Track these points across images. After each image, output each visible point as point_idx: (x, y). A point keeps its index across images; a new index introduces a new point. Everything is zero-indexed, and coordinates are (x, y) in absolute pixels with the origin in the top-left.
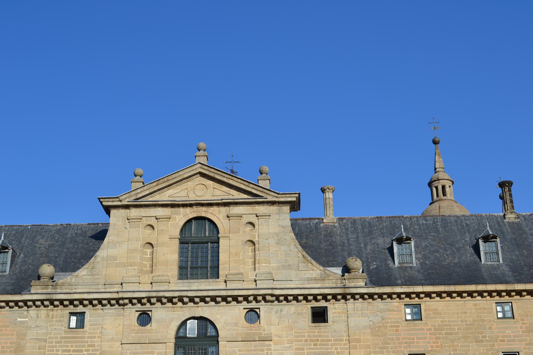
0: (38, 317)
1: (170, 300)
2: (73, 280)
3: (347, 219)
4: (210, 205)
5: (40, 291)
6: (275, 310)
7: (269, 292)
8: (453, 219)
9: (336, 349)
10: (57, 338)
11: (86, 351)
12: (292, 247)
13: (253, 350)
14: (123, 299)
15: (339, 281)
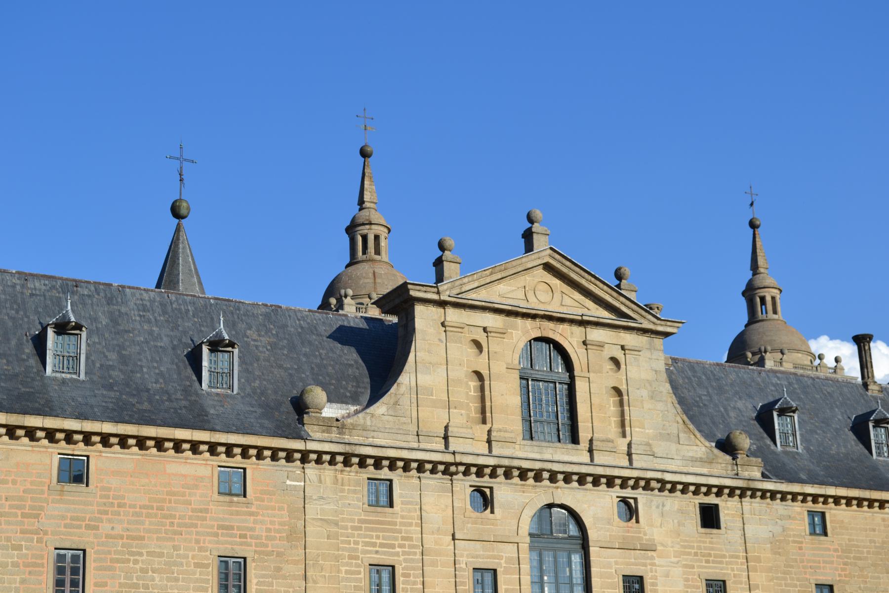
0: (320, 481)
1: (523, 474)
2: (369, 423)
3: (684, 360)
4: (561, 320)
5: (318, 435)
6: (654, 503)
7: (659, 475)
8: (810, 382)
9: (733, 570)
10: (353, 521)
11: (400, 546)
12: (670, 405)
13: (633, 564)
14: (457, 464)
15: (730, 467)
